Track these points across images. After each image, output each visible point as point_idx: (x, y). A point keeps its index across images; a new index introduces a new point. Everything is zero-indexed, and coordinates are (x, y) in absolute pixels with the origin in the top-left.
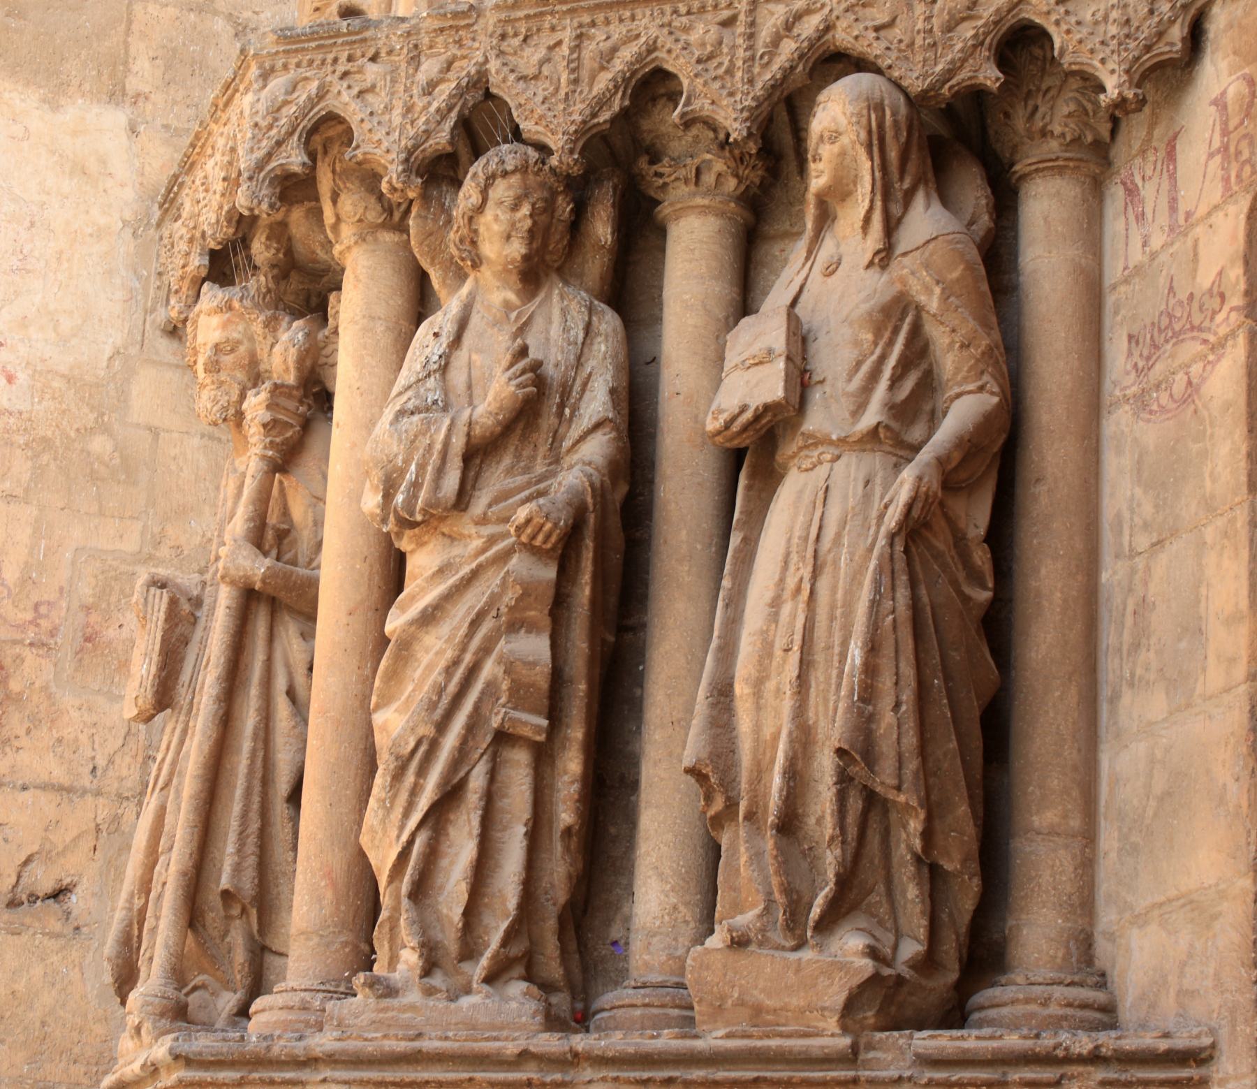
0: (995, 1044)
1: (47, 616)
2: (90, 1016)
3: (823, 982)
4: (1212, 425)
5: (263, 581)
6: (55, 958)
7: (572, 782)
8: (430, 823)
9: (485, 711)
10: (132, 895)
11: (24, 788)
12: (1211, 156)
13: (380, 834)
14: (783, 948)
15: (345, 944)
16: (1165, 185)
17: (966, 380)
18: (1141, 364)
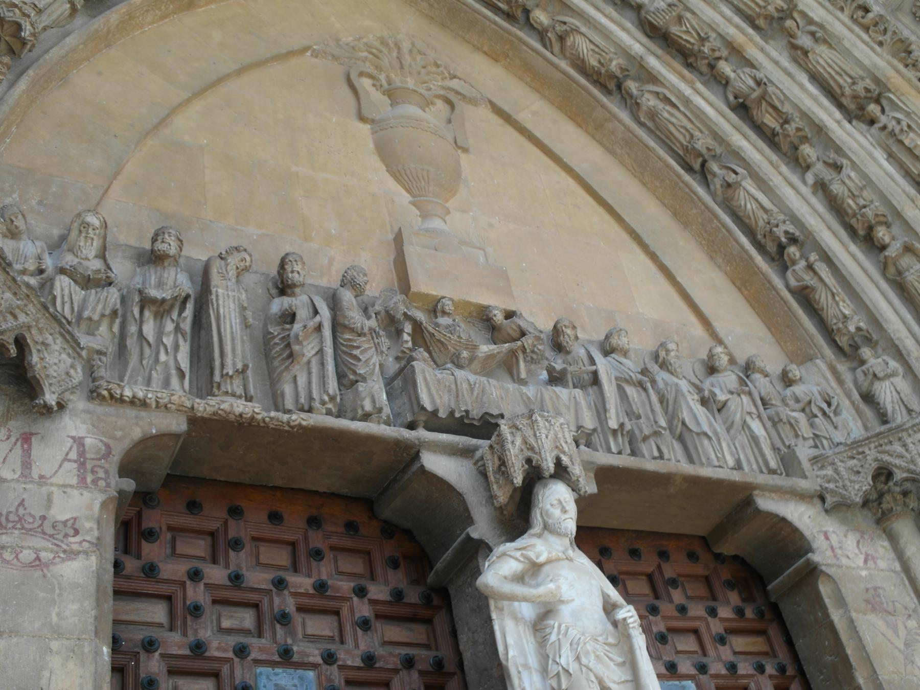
4: (60, 589)
16: (18, 451)
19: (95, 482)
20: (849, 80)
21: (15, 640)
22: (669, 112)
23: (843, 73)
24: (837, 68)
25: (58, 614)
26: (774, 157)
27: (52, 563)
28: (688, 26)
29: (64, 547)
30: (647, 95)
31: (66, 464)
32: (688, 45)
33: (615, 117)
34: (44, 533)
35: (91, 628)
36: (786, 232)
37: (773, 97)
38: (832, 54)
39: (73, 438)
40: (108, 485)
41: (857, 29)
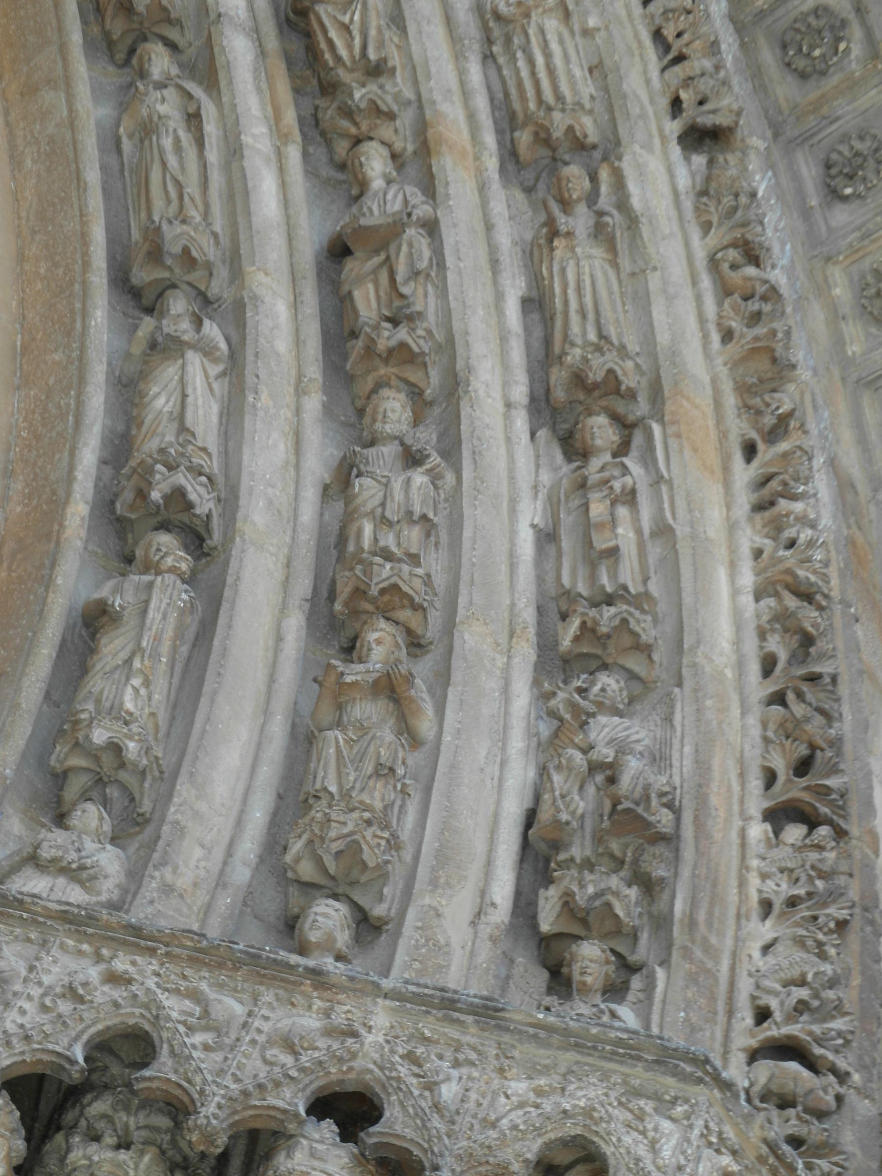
20: (592, 336)
22: (177, 140)
23: (591, 316)
24: (588, 299)
26: (314, 371)
28: (357, 17)
30: (170, 93)
32: (327, 56)
33: (68, 83)
36: (178, 495)
37: (405, 248)
38: (605, 273)
41: (706, 282)
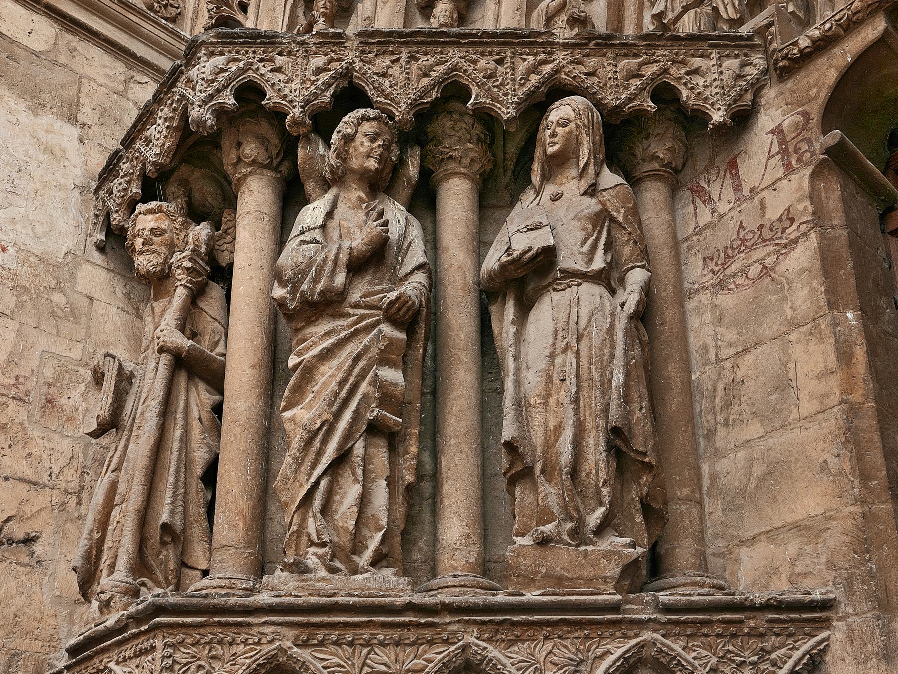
0: (710, 598)
1: (24, 384)
2: (46, 613)
3: (603, 562)
4: (788, 282)
5: (188, 351)
6: (23, 578)
7: (412, 459)
8: (330, 472)
9: (362, 411)
10: (92, 531)
11: (7, 478)
12: (770, 157)
13: (292, 480)
14: (571, 545)
15: (251, 554)
17: (636, 260)
18: (716, 269)
19: (799, 160)
21: (760, 350)
25: (791, 308)
27: (777, 263)
29: (784, 241)
31: (772, 162)
34: (764, 241)
35: (823, 303)
39: (772, 132)
40: (813, 153)
